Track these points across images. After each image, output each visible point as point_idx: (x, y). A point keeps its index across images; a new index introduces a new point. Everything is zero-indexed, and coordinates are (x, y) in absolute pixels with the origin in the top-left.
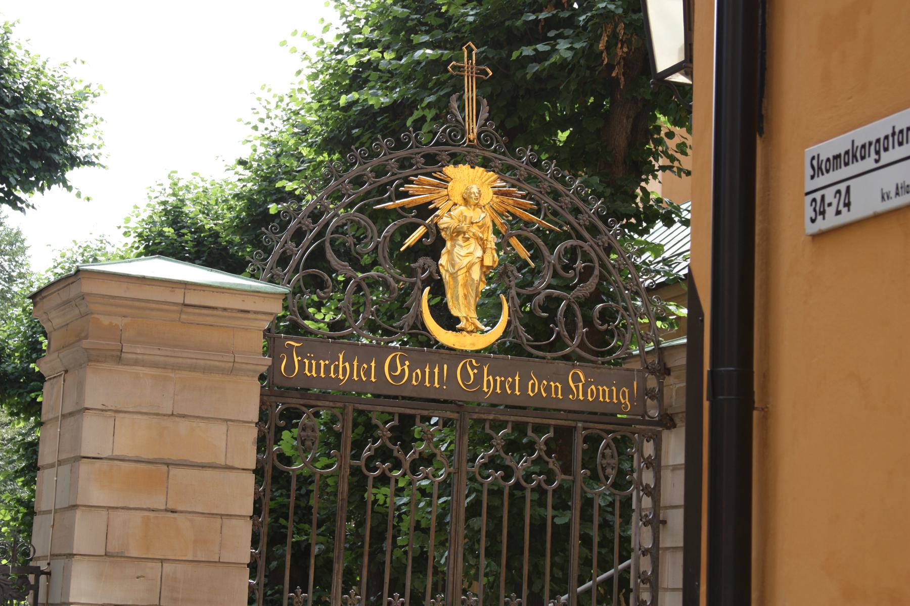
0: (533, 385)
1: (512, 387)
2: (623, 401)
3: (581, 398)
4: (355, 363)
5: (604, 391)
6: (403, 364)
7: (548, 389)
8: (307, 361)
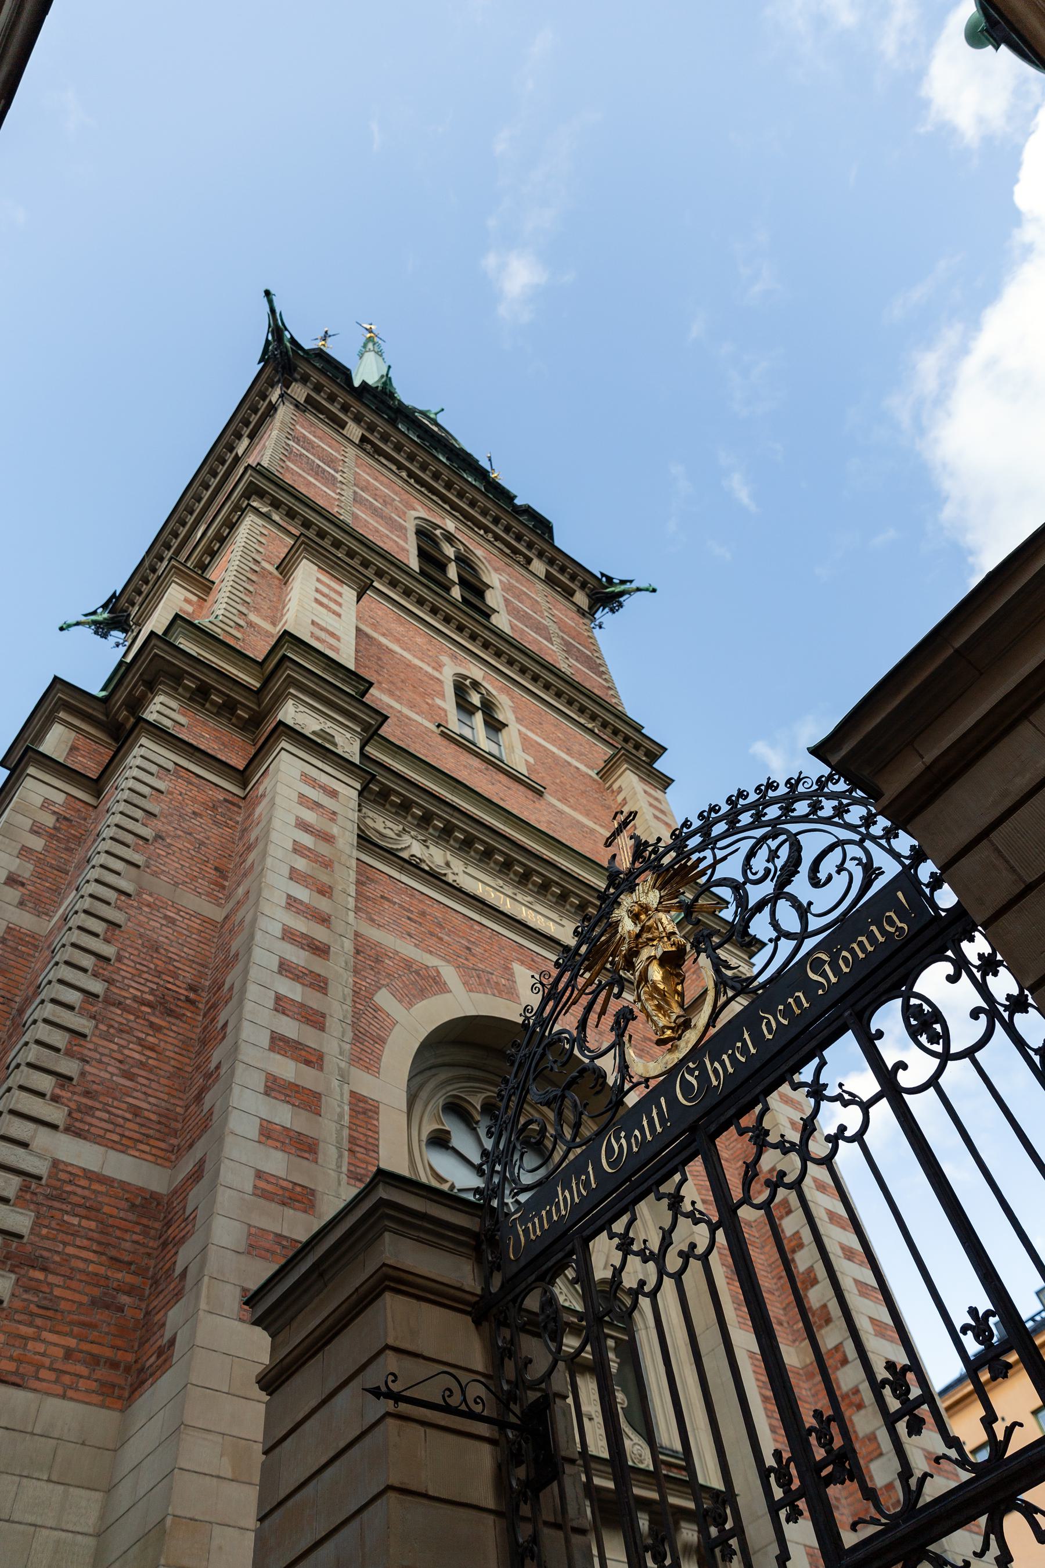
0: (769, 1024)
1: (745, 1050)
2: (892, 930)
3: (834, 980)
4: (574, 1185)
5: (861, 945)
6: (618, 1139)
7: (788, 1012)
8: (530, 1225)
